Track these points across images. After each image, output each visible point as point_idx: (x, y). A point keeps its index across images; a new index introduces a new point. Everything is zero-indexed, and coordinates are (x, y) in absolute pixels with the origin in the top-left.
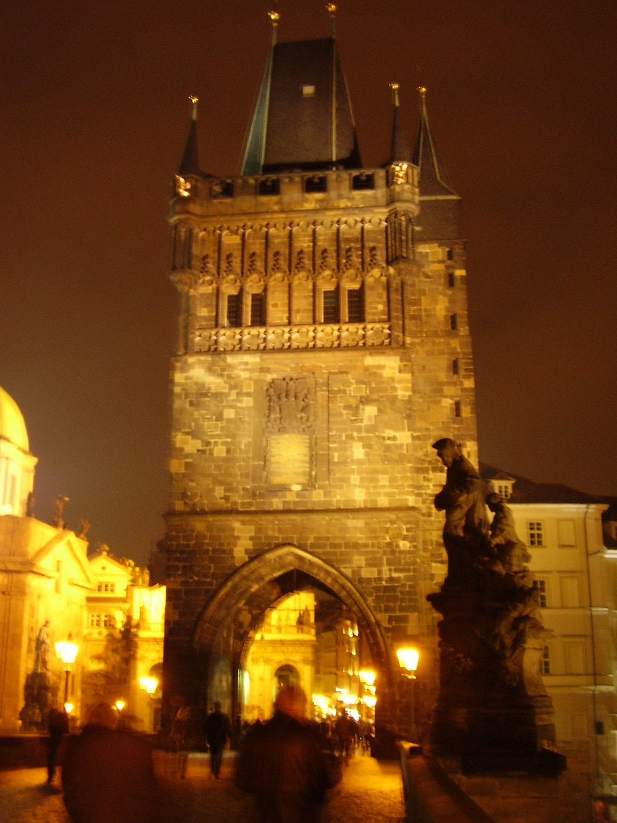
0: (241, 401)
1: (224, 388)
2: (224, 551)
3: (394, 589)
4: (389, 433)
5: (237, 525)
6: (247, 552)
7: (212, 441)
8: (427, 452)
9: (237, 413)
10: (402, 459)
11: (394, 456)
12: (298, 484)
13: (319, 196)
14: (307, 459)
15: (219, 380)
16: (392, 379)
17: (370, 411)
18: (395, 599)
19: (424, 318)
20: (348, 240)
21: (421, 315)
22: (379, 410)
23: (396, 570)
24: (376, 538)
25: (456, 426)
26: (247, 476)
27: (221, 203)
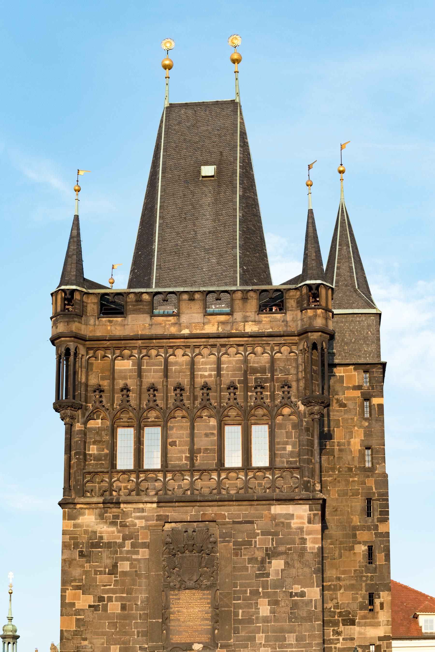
0: (137, 553)
1: (119, 538)
7: (106, 596)
8: (338, 603)
9: (131, 565)
11: (303, 613)
13: (222, 318)
16: (301, 529)
17: (277, 565)
20: (254, 371)
21: (334, 448)
25: (369, 574)
27: (110, 322)
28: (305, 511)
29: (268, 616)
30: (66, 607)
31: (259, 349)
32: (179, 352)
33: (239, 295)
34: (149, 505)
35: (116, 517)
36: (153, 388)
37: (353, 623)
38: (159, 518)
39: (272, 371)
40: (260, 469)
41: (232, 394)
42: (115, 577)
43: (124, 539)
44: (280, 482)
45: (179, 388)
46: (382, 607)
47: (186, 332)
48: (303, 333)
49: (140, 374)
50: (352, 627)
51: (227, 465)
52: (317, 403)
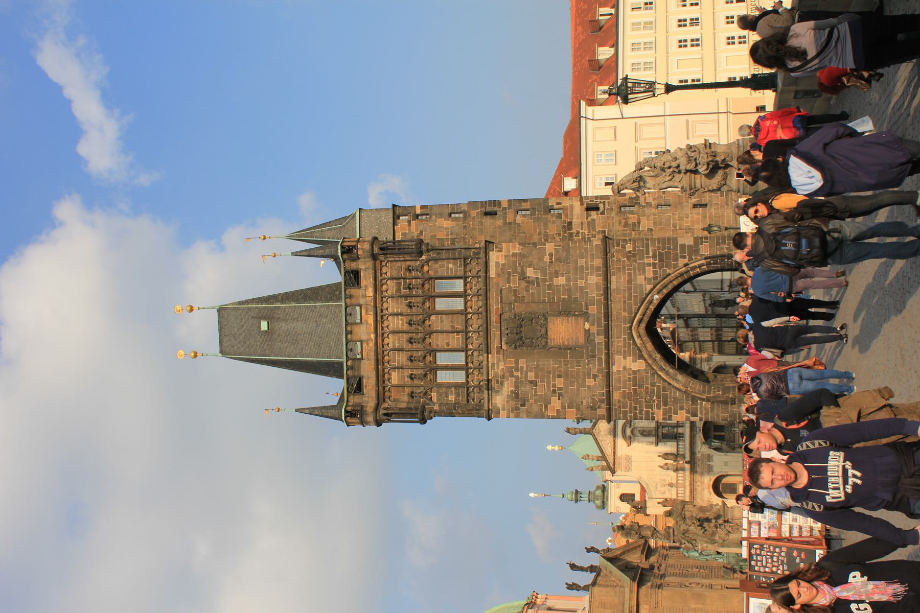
0: (522, 367)
2: (635, 378)
3: (660, 254)
5: (615, 368)
6: (634, 361)
10: (567, 250)
16: (506, 256)
17: (530, 272)
18: (668, 254)
19: (453, 237)
20: (399, 290)
22: (529, 266)
23: (648, 253)
24: (624, 268)
26: (578, 362)
31: (384, 287)
32: (386, 341)
33: (348, 300)
35: (498, 381)
36: (411, 360)
37: (570, 223)
38: (498, 353)
39: (399, 279)
43: (513, 376)
44: (474, 272)
45: (410, 341)
46: (560, 204)
47: (373, 336)
48: (374, 257)
49: (401, 368)
51: (462, 308)
52: (421, 246)
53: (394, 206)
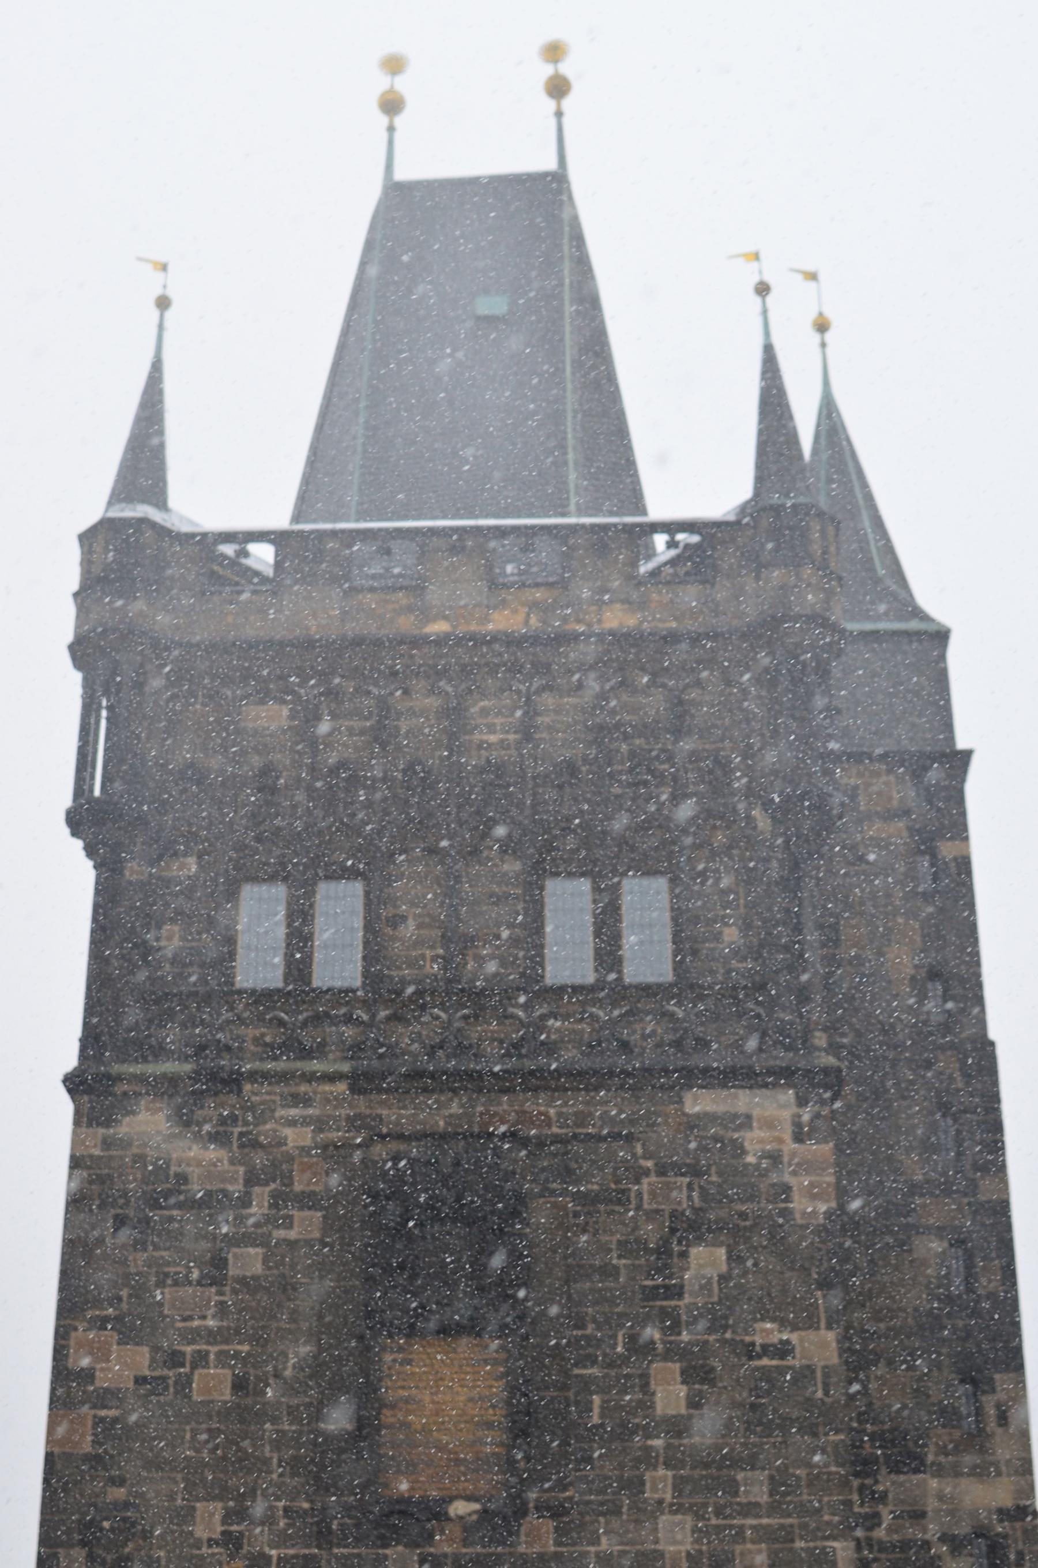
1: (234, 1180)
4: (768, 1332)
7: (189, 1349)
12: (469, 1498)
14: (497, 1416)
15: (213, 1153)
16: (775, 1158)
17: (705, 1262)
28: (784, 1106)
29: (682, 1416)
30: (68, 1385)
34: (327, 1088)
38: (353, 1122)
40: (647, 990)
41: (567, 790)
42: (221, 1293)
47: (438, 627)
50: (916, 1478)
53: (966, 756)
